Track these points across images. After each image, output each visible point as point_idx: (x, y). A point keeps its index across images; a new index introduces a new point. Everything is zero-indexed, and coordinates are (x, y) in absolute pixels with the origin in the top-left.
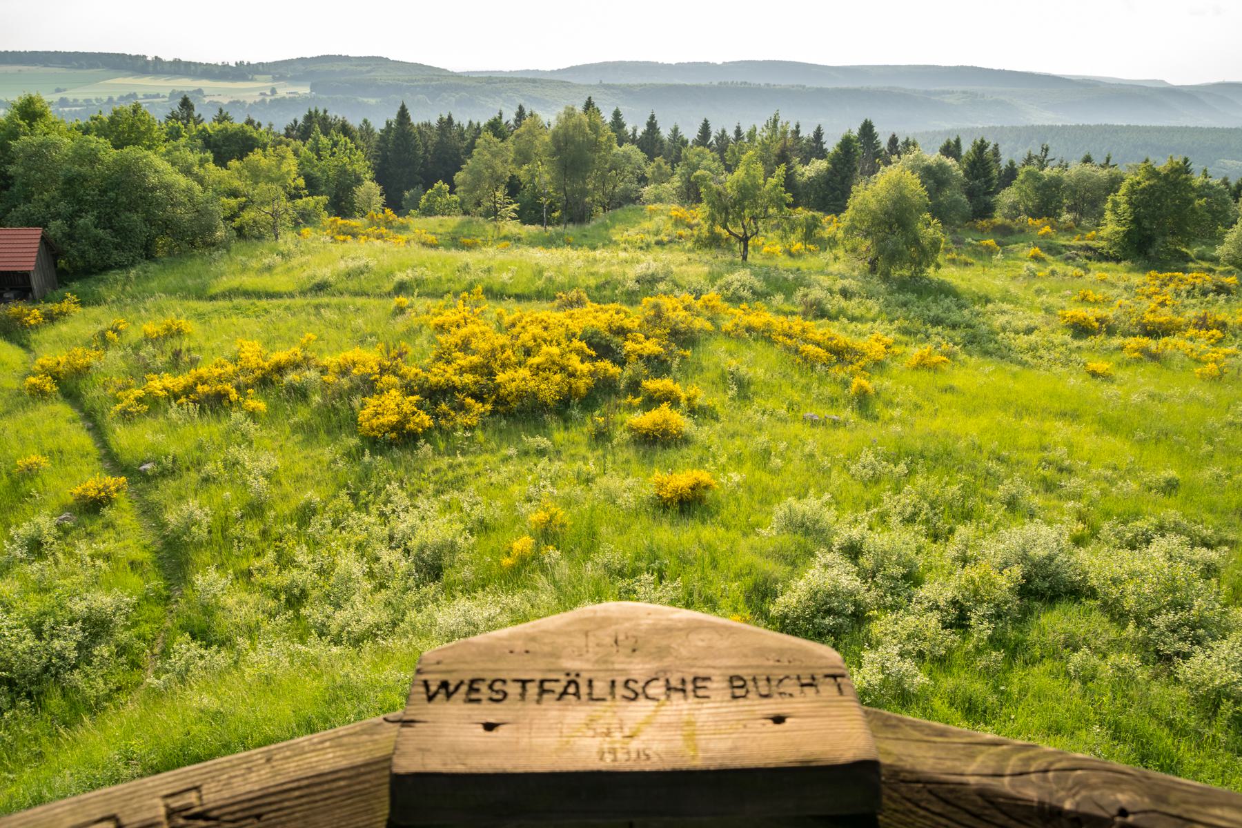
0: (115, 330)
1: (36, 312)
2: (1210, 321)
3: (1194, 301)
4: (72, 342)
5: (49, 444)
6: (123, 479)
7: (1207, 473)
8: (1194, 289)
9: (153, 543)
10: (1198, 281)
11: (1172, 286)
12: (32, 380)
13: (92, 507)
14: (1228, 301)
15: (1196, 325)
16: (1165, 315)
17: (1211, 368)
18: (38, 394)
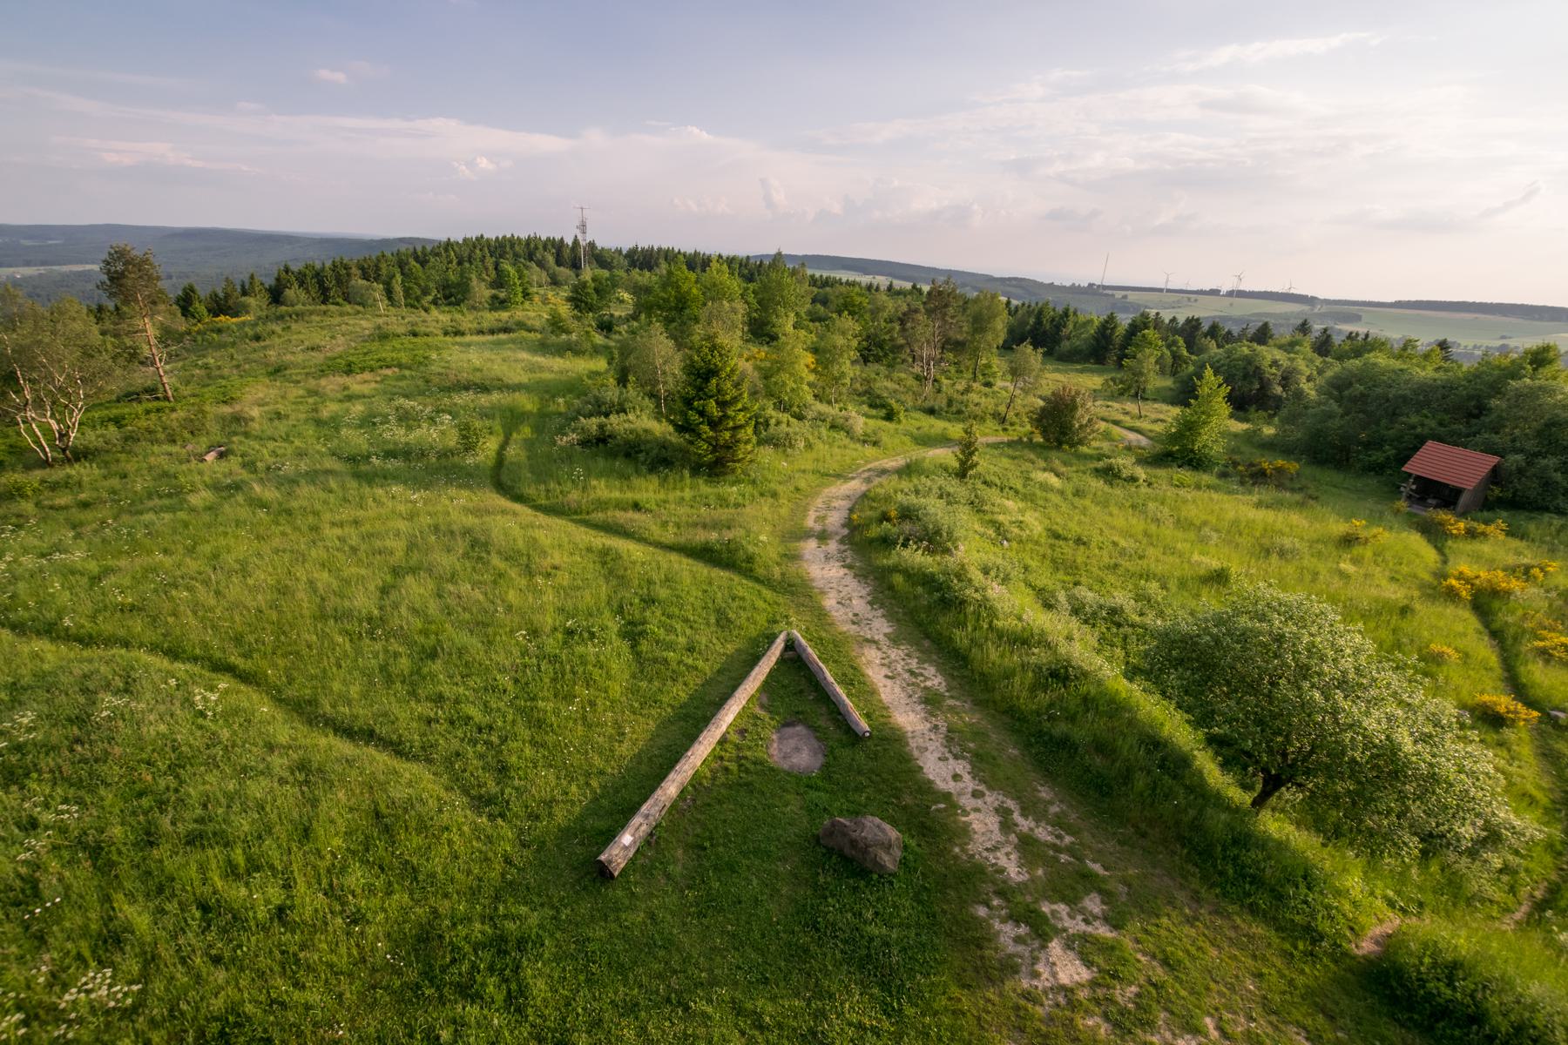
0: (1542, 569)
1: (1462, 525)
4: (1491, 564)
5: (1460, 643)
6: (1536, 714)
9: (1551, 790)
12: (1454, 582)
13: (1492, 720)
18: (1451, 595)
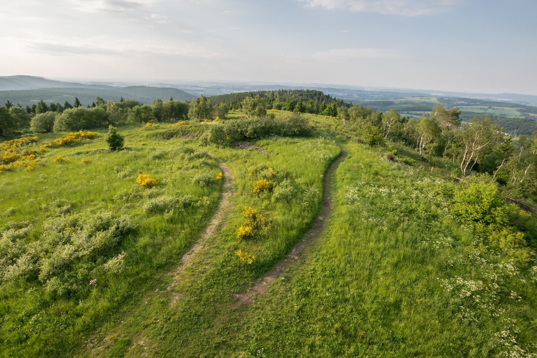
2: (29, 152)
3: (25, 147)
7: (27, 203)
8: (23, 143)
10: (23, 141)
11: (14, 144)
14: (37, 144)
15: (24, 155)
16: (12, 155)
17: (29, 168)
